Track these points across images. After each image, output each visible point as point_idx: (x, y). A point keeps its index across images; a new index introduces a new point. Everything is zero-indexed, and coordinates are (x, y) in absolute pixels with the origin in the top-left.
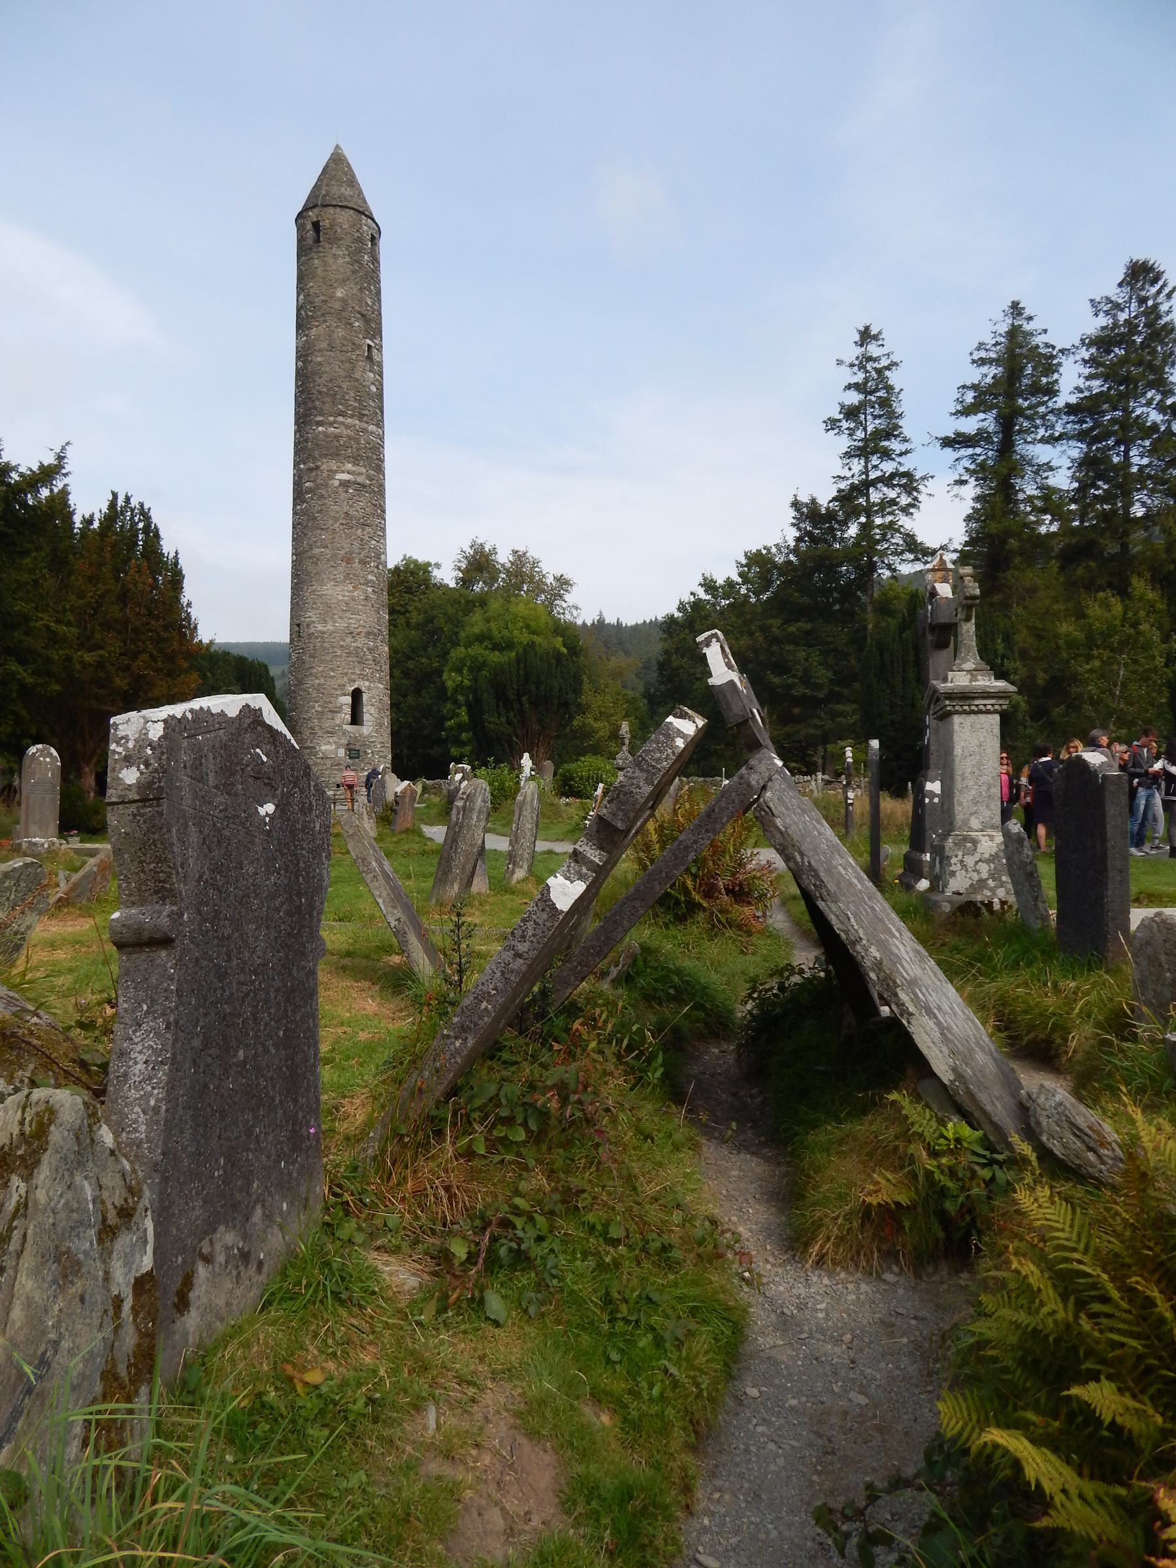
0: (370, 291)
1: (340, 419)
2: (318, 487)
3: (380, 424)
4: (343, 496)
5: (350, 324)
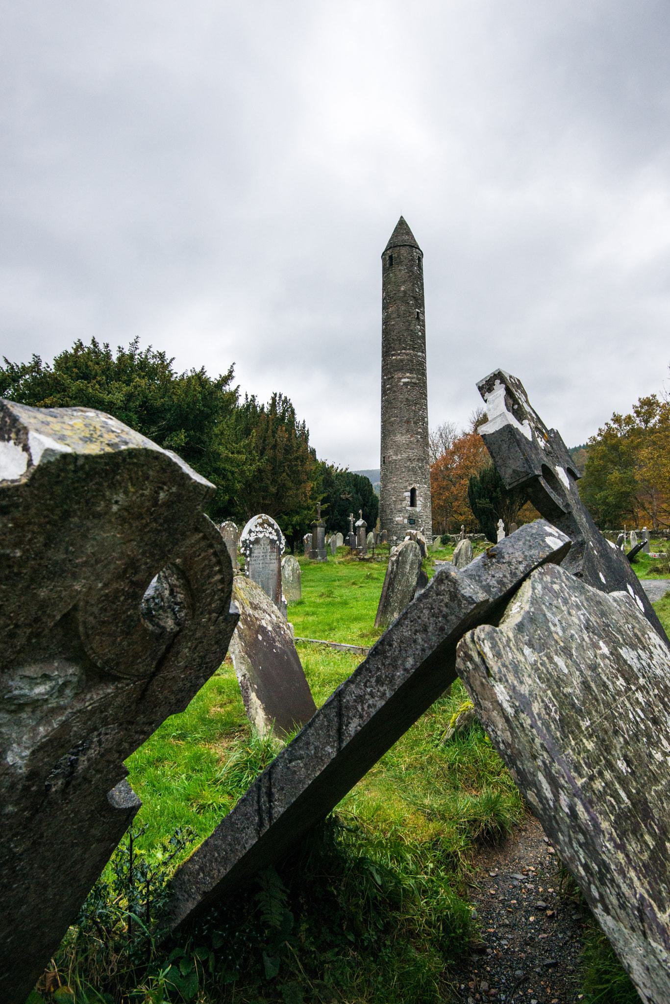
2: (393, 387)
3: (424, 351)
4: (405, 390)
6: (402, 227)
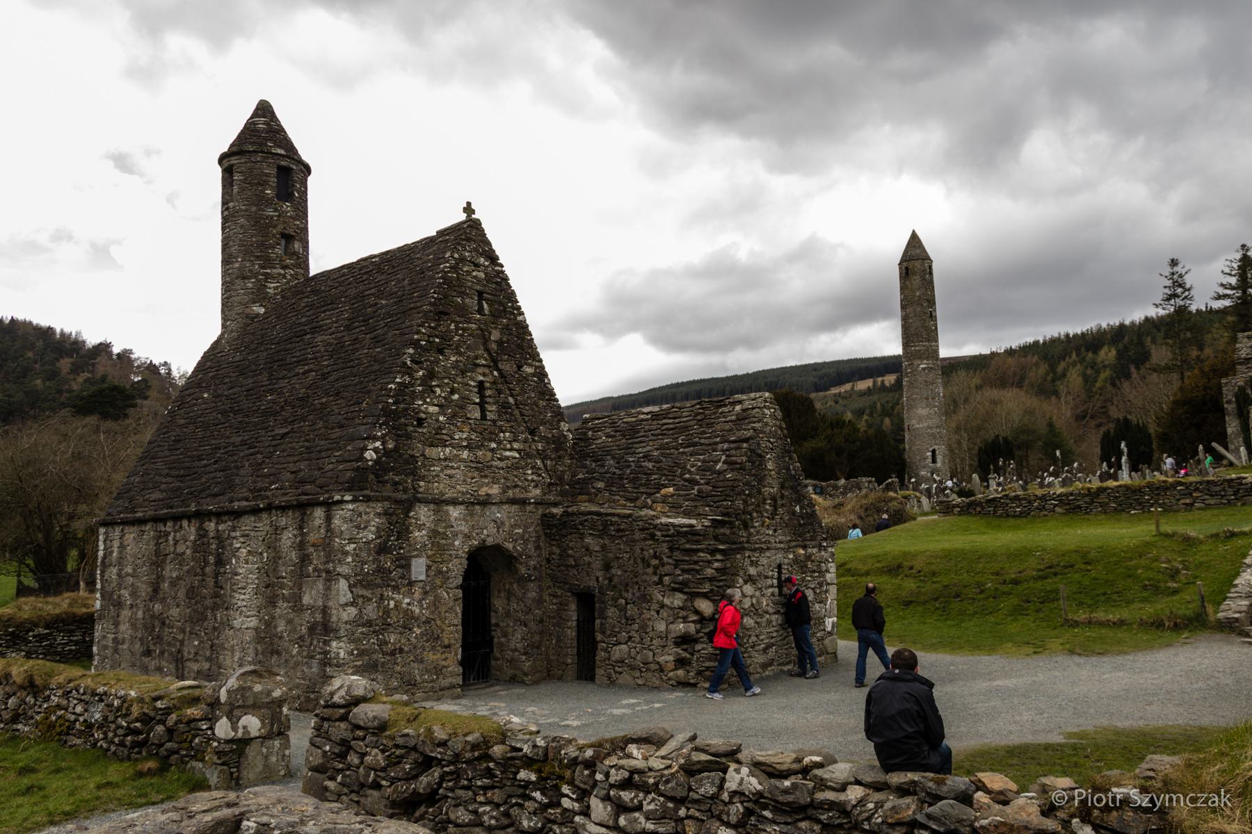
6: (914, 240)
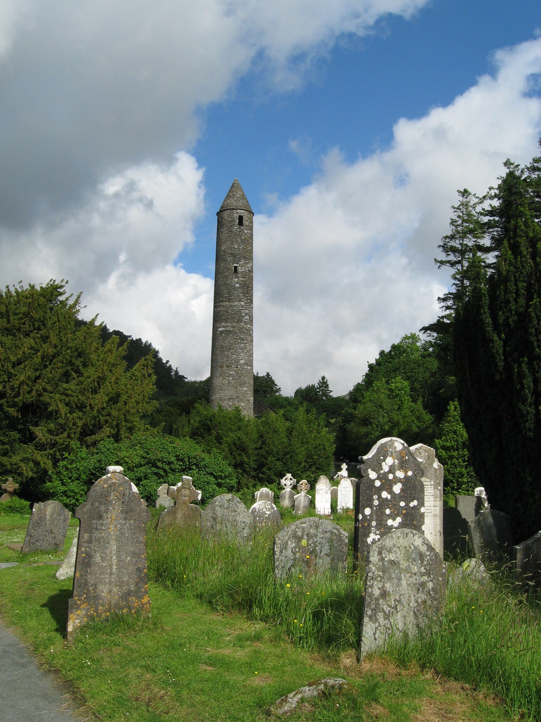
0: (237, 242)
1: (221, 304)
5: (226, 260)
